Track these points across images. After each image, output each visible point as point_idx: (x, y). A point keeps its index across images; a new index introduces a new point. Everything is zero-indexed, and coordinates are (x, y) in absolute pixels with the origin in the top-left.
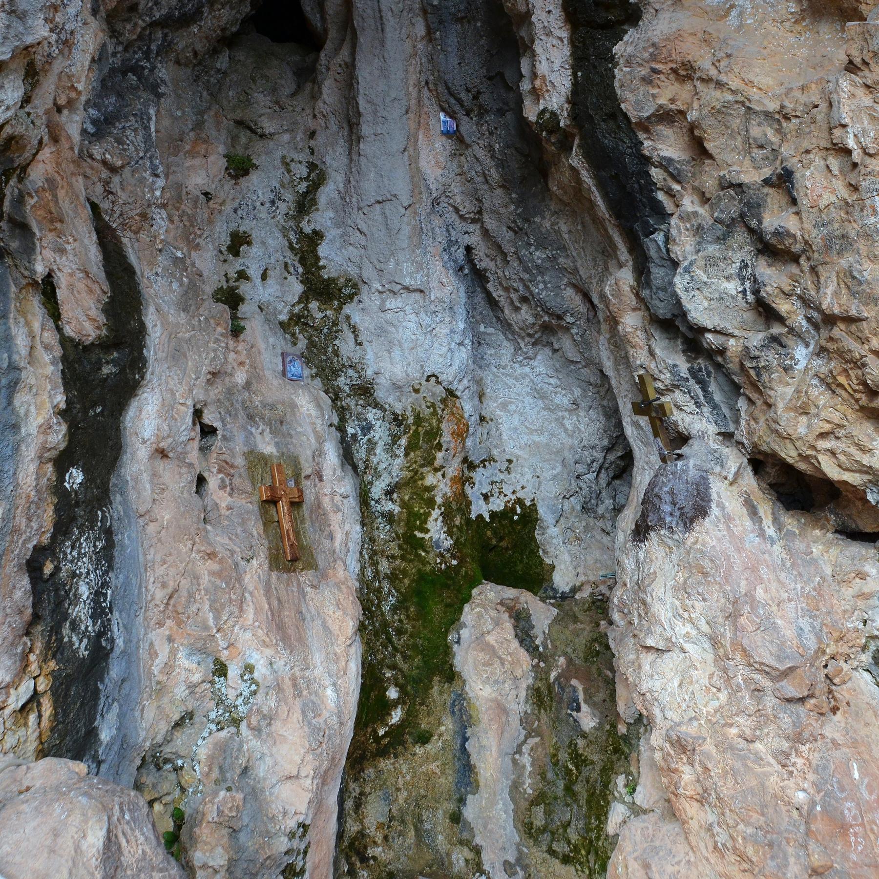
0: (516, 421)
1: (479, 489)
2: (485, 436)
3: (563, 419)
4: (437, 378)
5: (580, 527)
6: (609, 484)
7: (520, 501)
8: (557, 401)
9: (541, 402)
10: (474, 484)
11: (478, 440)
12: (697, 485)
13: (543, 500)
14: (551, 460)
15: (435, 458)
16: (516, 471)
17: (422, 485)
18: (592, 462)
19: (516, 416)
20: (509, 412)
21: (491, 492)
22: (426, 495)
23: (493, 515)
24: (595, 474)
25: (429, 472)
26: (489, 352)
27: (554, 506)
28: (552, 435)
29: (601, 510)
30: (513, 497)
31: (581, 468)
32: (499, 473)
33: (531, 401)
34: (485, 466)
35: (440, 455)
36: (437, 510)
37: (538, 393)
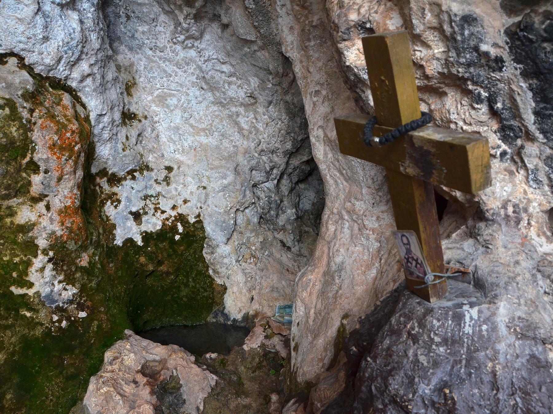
0: (177, 118)
1: (126, 207)
2: (133, 140)
3: (238, 116)
4: (21, 59)
5: (257, 241)
6: (291, 190)
7: (181, 218)
8: (231, 93)
9: (210, 94)
10: (119, 201)
11: (120, 146)
12: (526, 394)
13: (210, 216)
14: (221, 167)
15: (29, 183)
16: (176, 182)
17: (12, 223)
18: (272, 169)
19: (178, 113)
20: (168, 106)
21: (143, 208)
22: (20, 238)
23: (147, 237)
24: (276, 182)
25: (23, 203)
26: (140, 29)
27: (224, 222)
28: (223, 135)
29: (282, 220)
30: (174, 213)
31: (258, 176)
32: (155, 185)
33: (198, 93)
34: (134, 178)
35: (36, 179)
36: (41, 257)
37: (207, 83)
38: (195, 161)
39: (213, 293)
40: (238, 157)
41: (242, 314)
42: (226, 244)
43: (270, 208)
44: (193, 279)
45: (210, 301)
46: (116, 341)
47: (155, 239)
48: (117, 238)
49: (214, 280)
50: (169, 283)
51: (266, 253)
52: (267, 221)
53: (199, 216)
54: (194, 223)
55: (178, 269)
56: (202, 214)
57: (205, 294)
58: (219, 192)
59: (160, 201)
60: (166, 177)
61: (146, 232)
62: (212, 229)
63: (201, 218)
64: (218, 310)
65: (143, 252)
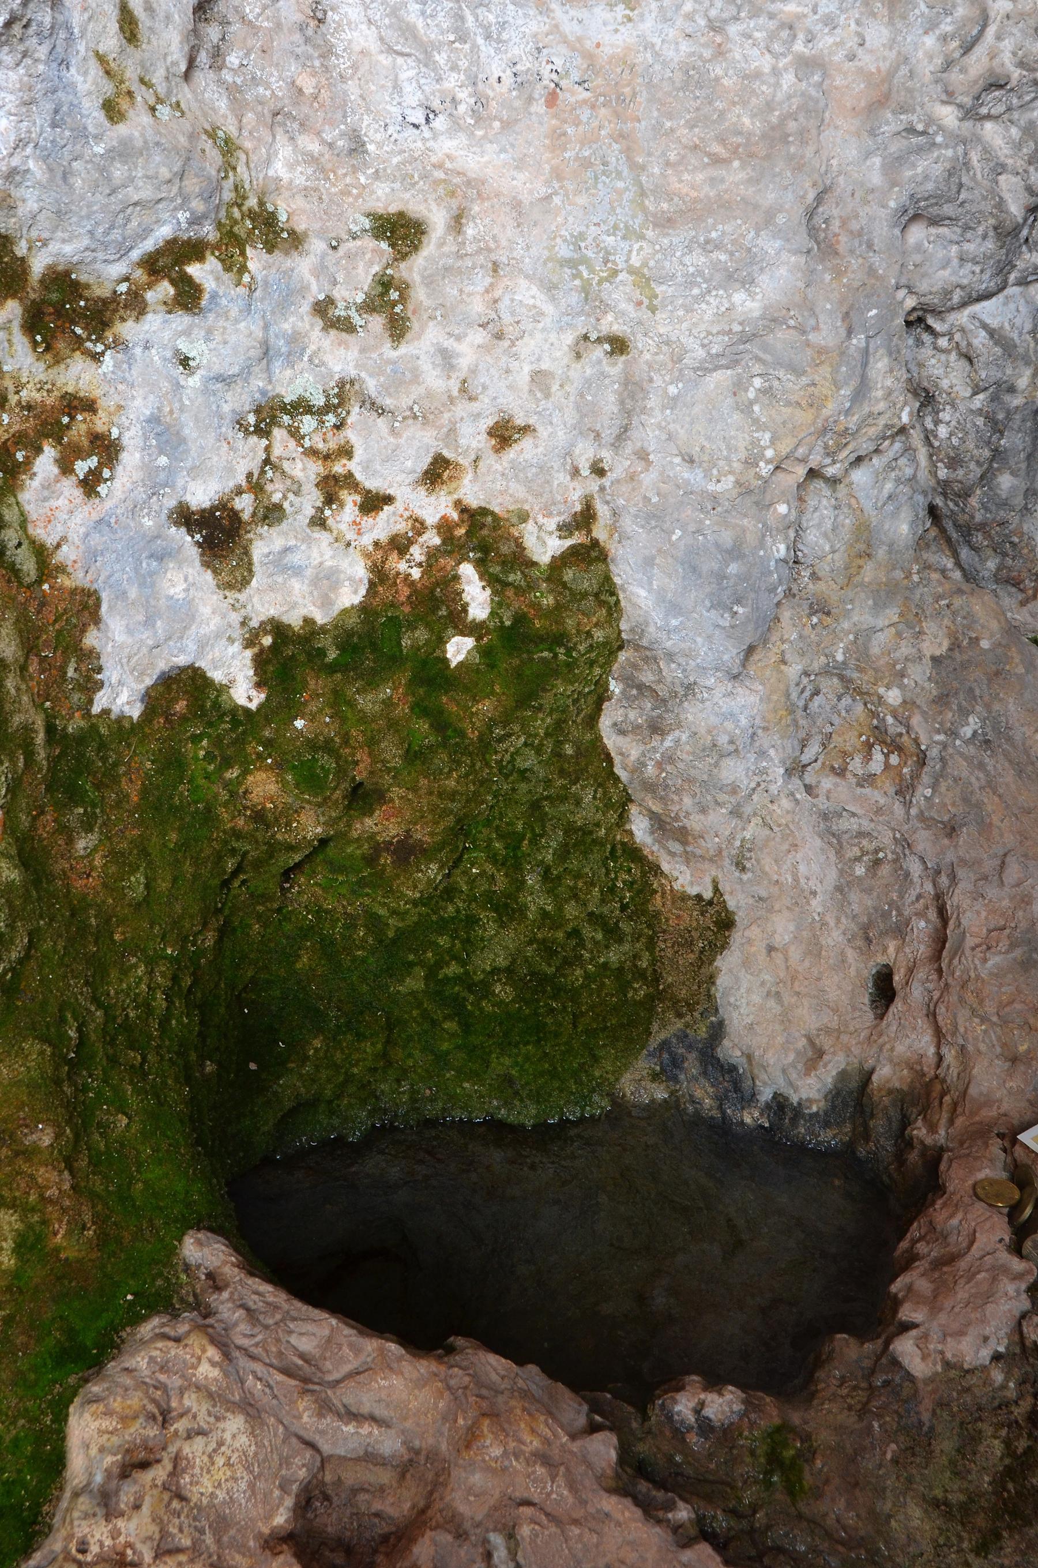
14: (724, 206)
16: (446, 313)
21: (256, 486)
27: (735, 552)
32: (317, 338)
38: (557, 174)
39: (651, 944)
40: (828, 134)
41: (826, 1076)
42: (735, 677)
43: (997, 453)
44: (546, 873)
45: (640, 991)
46: (137, 1320)
47: (332, 669)
48: (111, 674)
49: (656, 869)
50: (415, 903)
51: (971, 726)
52: (966, 530)
53: (585, 518)
54: (560, 562)
55: (461, 829)
56: (602, 510)
57: (613, 956)
58: (704, 369)
59: (350, 434)
60: (385, 284)
61: (278, 628)
62: (661, 597)
63: (599, 532)
64: (682, 1037)
65: (268, 743)
